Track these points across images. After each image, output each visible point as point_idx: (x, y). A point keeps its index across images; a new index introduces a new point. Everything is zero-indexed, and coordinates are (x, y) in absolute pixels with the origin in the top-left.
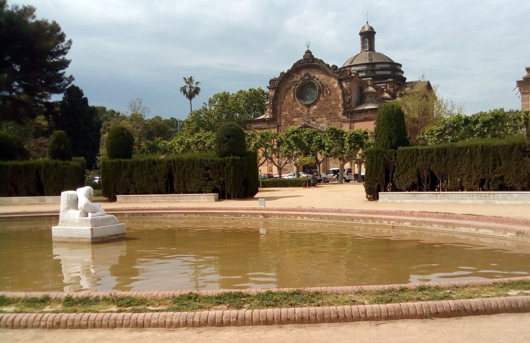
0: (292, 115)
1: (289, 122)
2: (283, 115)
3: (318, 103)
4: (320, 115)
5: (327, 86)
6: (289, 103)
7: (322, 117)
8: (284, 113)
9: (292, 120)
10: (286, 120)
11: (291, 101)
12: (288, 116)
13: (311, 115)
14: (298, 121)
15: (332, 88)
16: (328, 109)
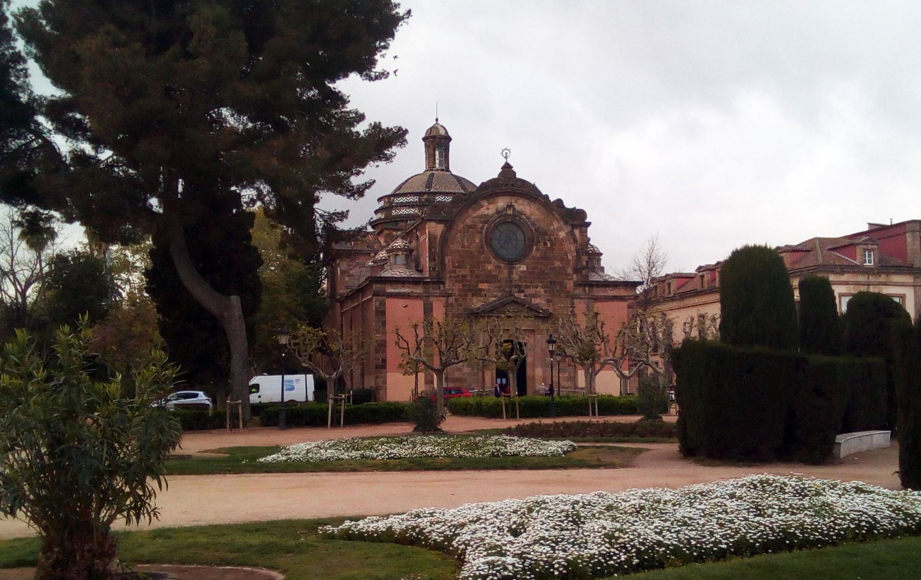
0: (477, 277)
6: (471, 253)
8: (460, 272)
9: (477, 286)
10: (463, 286)
13: (515, 280)
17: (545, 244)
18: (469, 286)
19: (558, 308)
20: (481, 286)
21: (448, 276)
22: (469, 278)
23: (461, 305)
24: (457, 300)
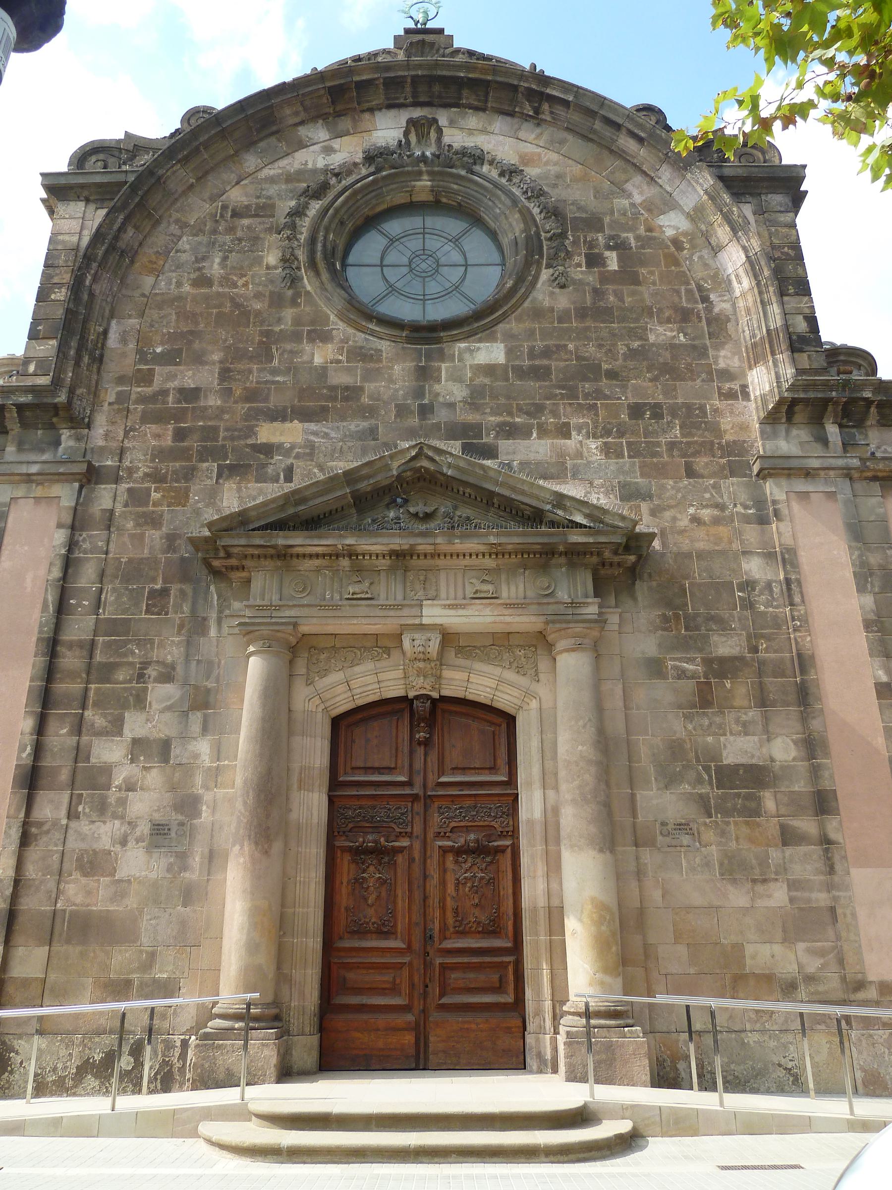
0: (251, 396)
1: (205, 454)
2: (164, 393)
3: (512, 325)
4: (539, 409)
5: (594, 223)
6: (237, 305)
7: (564, 431)
8: (172, 377)
9: (251, 432)
10: (180, 435)
11: (258, 296)
12: (213, 401)
13: (451, 406)
14: (311, 446)
15: (638, 238)
16: (612, 375)
17: (594, 260)
18: (210, 433)
19: (684, 522)
20: (267, 433)
21: (111, 397)
22: (213, 401)
23: (154, 521)
24: (137, 497)
